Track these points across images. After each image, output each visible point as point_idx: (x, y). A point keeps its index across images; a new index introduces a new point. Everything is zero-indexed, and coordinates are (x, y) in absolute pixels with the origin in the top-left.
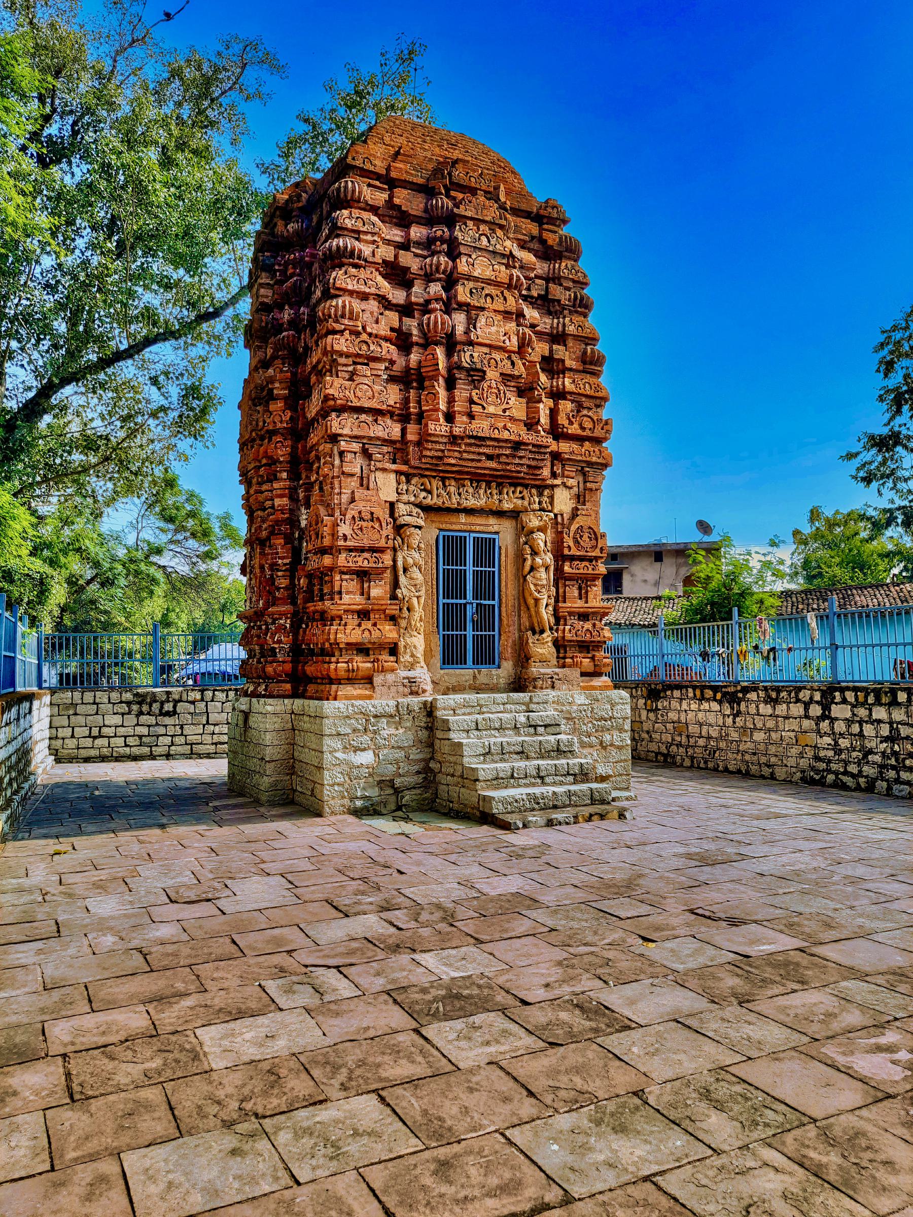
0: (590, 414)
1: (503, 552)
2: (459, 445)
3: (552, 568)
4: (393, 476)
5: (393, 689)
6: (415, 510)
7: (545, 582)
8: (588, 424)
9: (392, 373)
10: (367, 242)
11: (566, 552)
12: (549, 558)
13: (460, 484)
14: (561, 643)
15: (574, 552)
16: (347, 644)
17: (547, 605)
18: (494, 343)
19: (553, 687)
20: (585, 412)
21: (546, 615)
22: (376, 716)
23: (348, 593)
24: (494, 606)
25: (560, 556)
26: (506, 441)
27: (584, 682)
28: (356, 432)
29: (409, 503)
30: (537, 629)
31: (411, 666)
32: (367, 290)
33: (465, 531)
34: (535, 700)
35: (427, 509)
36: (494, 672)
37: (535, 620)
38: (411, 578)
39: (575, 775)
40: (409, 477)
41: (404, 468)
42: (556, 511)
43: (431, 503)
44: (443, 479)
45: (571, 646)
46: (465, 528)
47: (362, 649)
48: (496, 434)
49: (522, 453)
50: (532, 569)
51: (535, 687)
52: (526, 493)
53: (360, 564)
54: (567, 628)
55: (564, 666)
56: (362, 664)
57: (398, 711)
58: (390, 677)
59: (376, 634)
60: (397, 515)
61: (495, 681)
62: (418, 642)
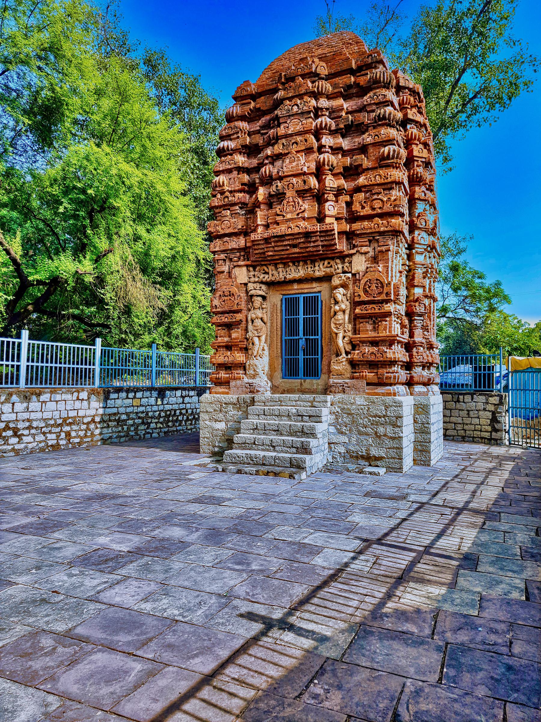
0: (380, 197)
2: (270, 243)
3: (347, 312)
4: (245, 269)
5: (240, 389)
6: (258, 286)
7: (341, 322)
8: (377, 204)
9: (248, 209)
10: (235, 139)
11: (357, 299)
13: (286, 265)
14: (354, 362)
15: (364, 298)
16: (219, 364)
17: (344, 337)
18: (294, 173)
20: (375, 197)
22: (226, 404)
23: (220, 337)
25: (355, 304)
26: (299, 234)
27: (368, 389)
28: (222, 248)
29: (255, 282)
31: (254, 376)
32: (230, 167)
33: (299, 294)
34: (316, 399)
35: (270, 284)
36: (315, 381)
39: (297, 448)
40: (254, 268)
41: (249, 263)
42: (353, 272)
43: (268, 280)
44: (276, 265)
46: (297, 291)
48: (290, 231)
49: (314, 239)
51: (331, 392)
52: (332, 263)
56: (223, 375)
57: (238, 401)
58: (239, 382)
61: (315, 387)
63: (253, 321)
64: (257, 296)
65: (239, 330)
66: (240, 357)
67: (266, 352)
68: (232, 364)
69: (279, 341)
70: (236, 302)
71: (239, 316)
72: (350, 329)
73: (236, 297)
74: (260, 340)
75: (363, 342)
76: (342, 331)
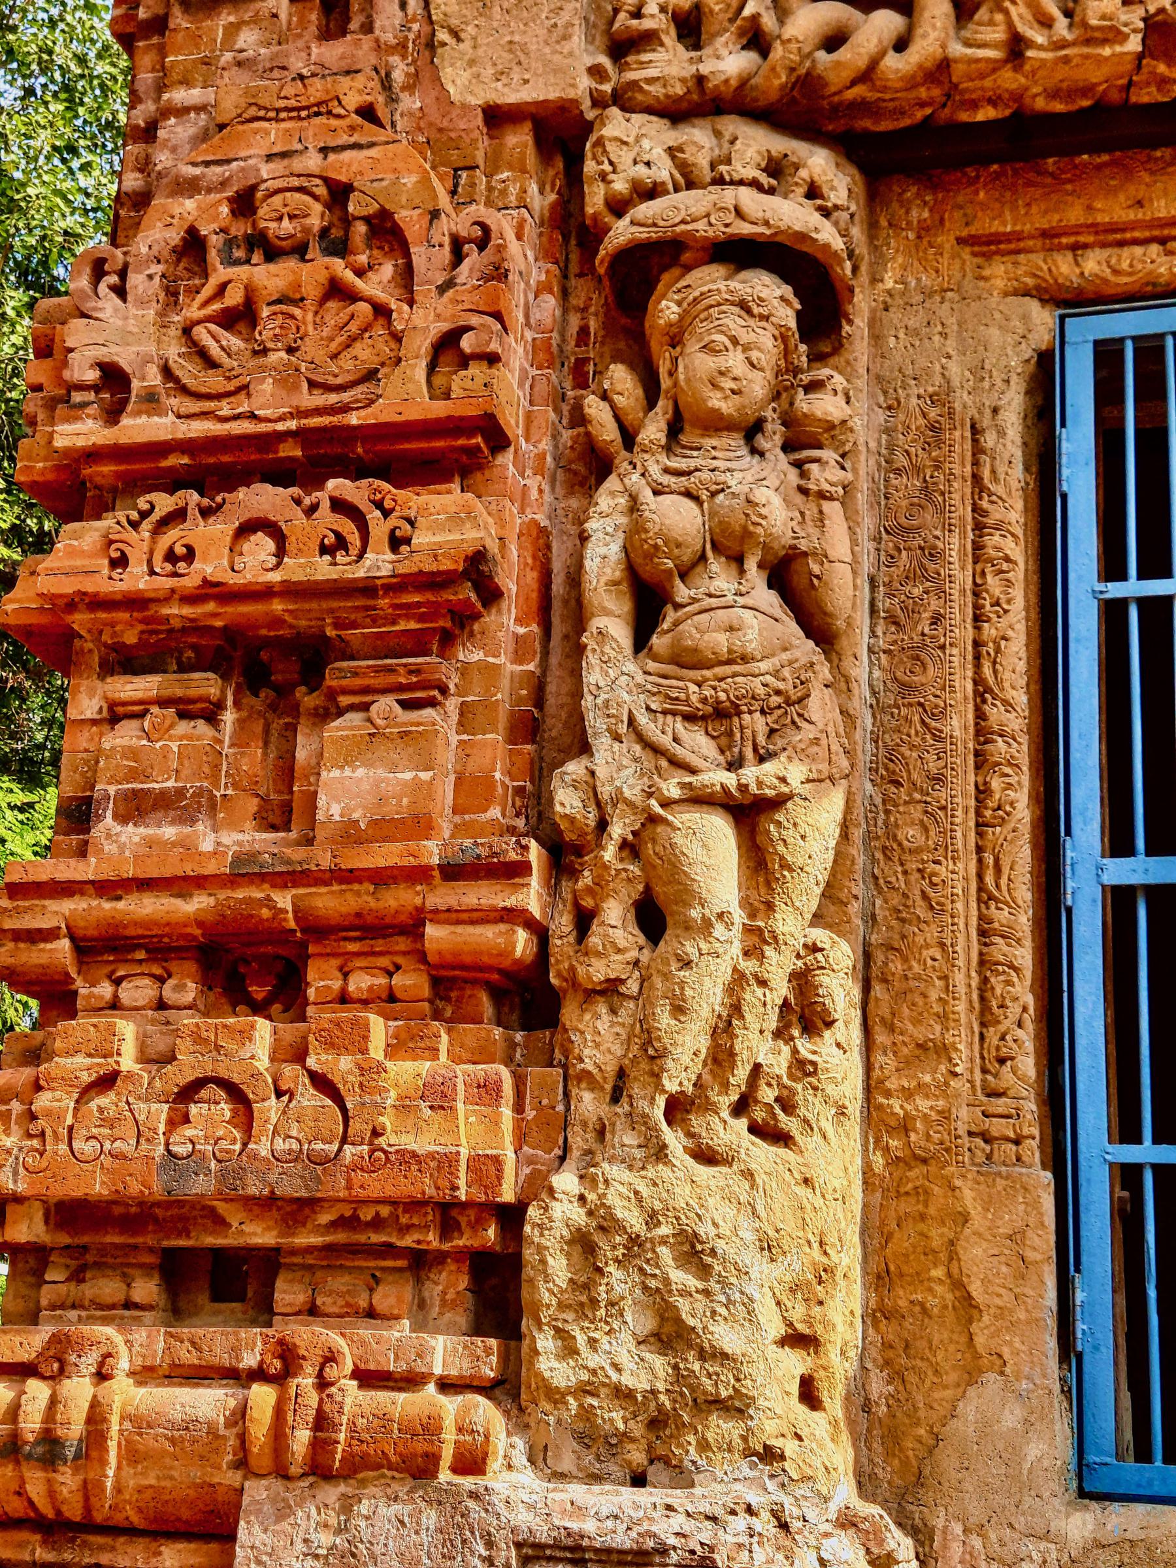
16: (69, 1214)
29: (699, 104)
38: (687, 660)
47: (194, 1261)
53: (210, 567)
59: (288, 1128)
60: (595, 200)
62: (781, 1223)
63: (649, 601)
64: (740, 253)
65: (442, 720)
66: (434, 1106)
67: (839, 1056)
68: (293, 1211)
69: (1019, 914)
70: (425, 321)
71: (444, 522)
73: (429, 260)
74: (760, 863)
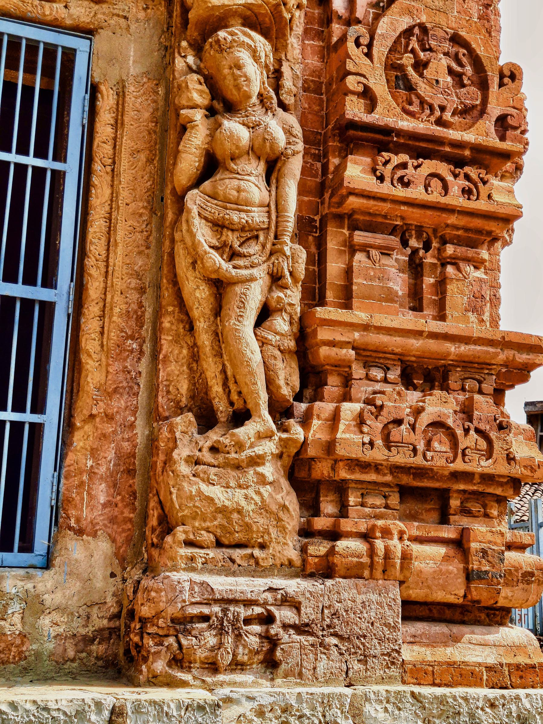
1: (107, 102)
3: (295, 167)
7: (258, 216)
12: (281, 129)
14: (322, 470)
17: (265, 314)
19: (271, 664)
21: (258, 355)
24: (47, 308)
25: (335, 135)
30: (222, 407)
37: (211, 368)
45: (367, 489)
50: (212, 165)
54: (350, 409)
55: (326, 570)
72: (301, 269)
75: (369, 356)
76: (260, 273)
